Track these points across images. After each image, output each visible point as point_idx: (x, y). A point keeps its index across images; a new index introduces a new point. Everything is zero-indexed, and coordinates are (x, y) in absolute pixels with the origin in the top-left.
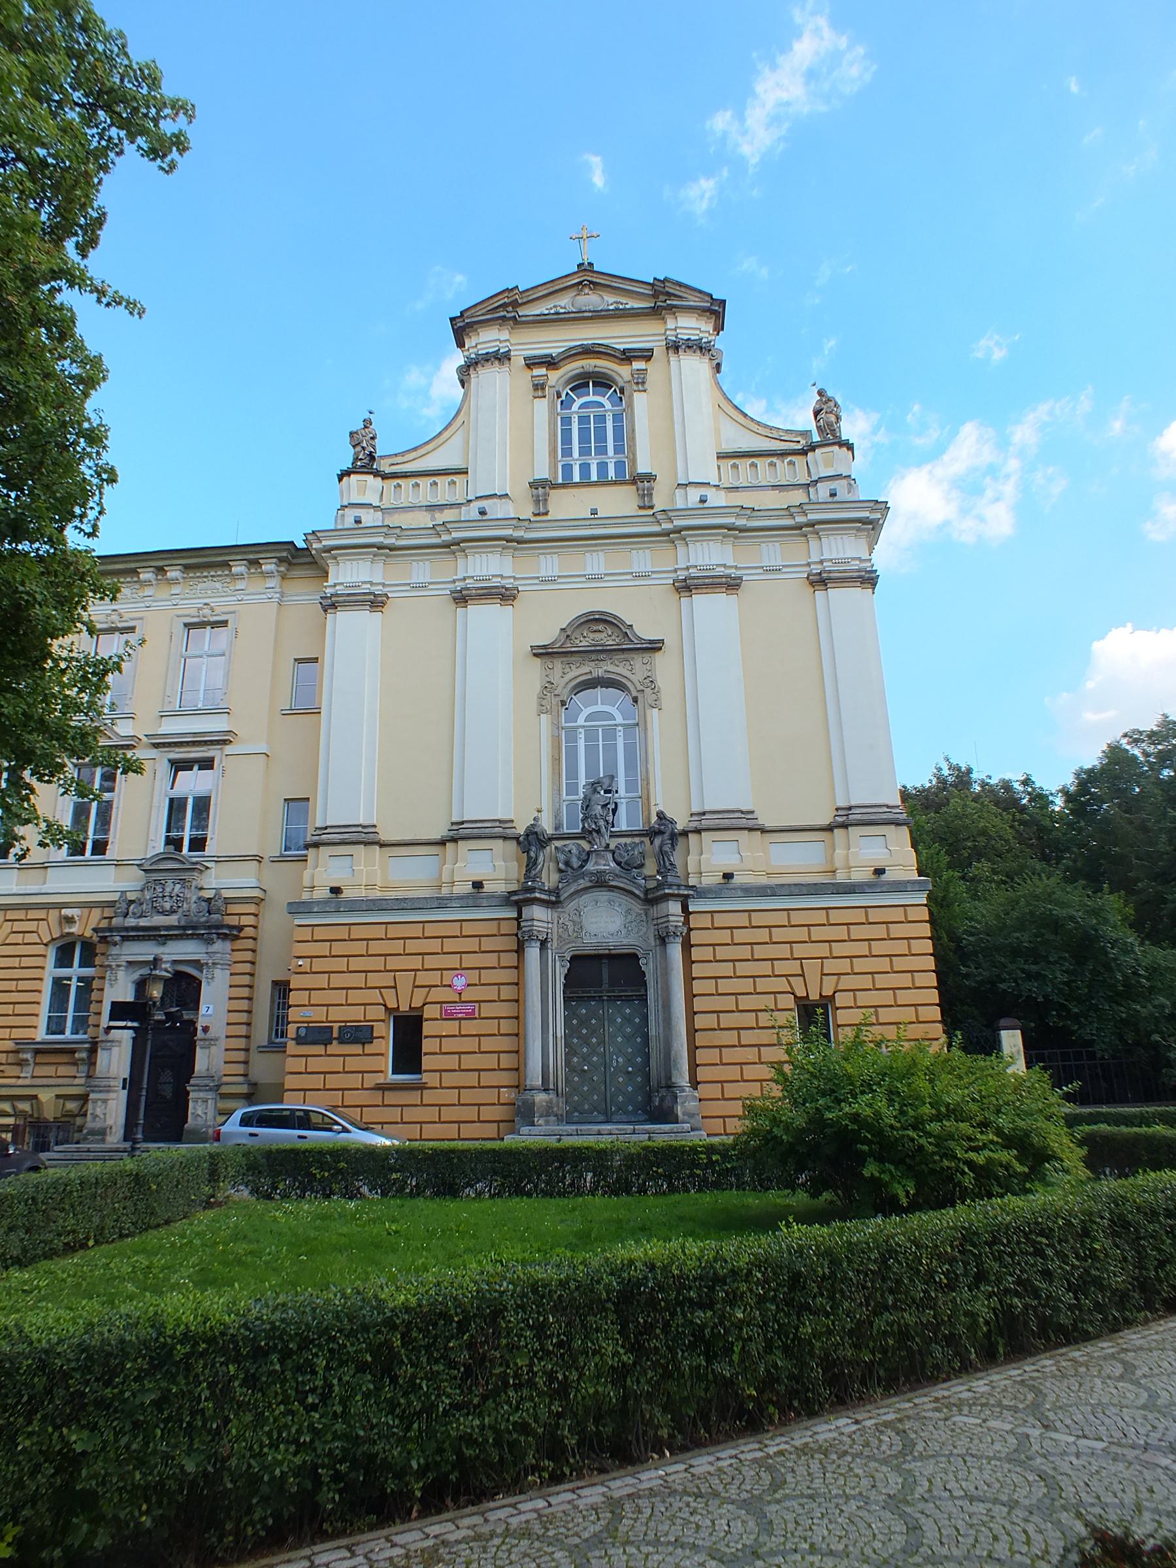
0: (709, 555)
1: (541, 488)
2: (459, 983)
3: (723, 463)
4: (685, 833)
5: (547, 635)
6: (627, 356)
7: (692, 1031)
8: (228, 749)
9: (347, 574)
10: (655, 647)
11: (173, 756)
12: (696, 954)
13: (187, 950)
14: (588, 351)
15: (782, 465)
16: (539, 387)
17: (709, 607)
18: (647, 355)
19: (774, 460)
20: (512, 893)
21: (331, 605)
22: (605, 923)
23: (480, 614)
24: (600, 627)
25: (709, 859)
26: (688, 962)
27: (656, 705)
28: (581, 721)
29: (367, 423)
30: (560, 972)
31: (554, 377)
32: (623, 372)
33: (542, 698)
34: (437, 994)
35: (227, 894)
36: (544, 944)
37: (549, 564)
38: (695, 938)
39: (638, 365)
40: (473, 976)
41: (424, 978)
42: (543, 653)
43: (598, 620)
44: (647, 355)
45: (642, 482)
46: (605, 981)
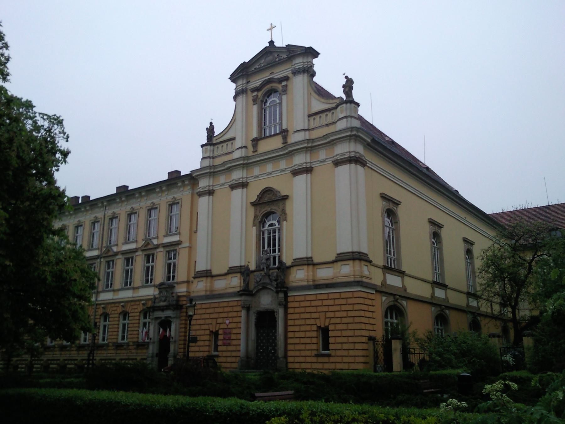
1: (256, 141)
2: (227, 322)
3: (312, 119)
4: (289, 267)
5: (254, 198)
6: (280, 81)
7: (286, 338)
8: (180, 246)
9: (203, 183)
10: (286, 198)
11: (167, 249)
12: (290, 311)
13: (169, 313)
14: (270, 81)
15: (329, 114)
16: (255, 101)
17: (302, 179)
18: (287, 79)
19: (327, 113)
20: (239, 292)
21: (200, 194)
22: (266, 301)
23: (238, 192)
24: (269, 193)
25: (299, 276)
26: (286, 313)
28: (266, 227)
29: (211, 123)
30: (253, 318)
31: (260, 94)
32: (279, 87)
33: (254, 221)
34: (222, 326)
35: (179, 294)
36: (248, 309)
37: (256, 171)
38: (290, 305)
39: (284, 83)
40: (231, 320)
41: (220, 321)
42: (254, 204)
43: (267, 191)
45: (284, 133)
46: (265, 321)
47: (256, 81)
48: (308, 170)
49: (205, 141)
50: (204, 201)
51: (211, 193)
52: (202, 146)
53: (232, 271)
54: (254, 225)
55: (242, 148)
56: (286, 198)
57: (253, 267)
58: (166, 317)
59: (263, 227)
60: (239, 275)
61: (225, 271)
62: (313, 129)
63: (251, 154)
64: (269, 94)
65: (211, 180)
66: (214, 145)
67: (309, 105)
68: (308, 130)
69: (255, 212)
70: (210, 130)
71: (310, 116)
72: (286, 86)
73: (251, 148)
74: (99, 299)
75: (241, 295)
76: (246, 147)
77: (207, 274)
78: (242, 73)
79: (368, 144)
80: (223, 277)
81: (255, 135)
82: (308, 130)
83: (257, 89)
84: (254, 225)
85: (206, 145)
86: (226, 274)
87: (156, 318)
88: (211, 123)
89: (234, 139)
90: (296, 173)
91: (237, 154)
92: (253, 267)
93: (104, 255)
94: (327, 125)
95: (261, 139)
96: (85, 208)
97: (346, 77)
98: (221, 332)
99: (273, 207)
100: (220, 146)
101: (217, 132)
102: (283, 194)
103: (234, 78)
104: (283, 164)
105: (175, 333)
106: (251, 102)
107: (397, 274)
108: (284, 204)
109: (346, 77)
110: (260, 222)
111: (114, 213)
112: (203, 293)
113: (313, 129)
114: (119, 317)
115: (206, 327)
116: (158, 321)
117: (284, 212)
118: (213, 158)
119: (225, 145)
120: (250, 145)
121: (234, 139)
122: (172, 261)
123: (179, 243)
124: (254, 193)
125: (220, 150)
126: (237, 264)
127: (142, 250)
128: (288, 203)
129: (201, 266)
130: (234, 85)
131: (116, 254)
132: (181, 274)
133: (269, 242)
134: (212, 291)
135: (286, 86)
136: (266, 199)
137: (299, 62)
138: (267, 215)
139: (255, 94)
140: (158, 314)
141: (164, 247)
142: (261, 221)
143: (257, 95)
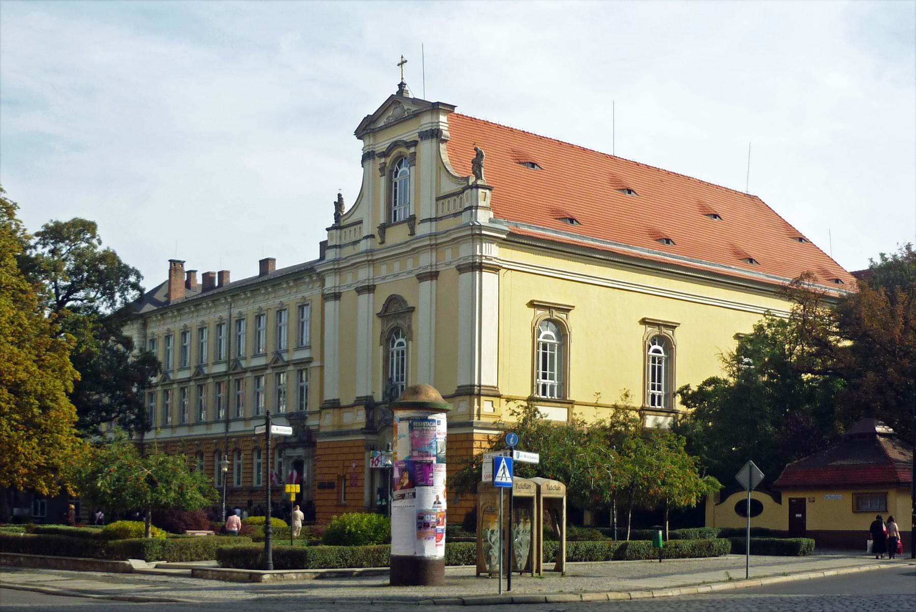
0: (426, 260)
1: (383, 228)
2: (354, 465)
5: (379, 309)
8: (312, 365)
13: (300, 452)
14: (395, 145)
16: (382, 169)
18: (415, 143)
19: (455, 197)
23: (364, 298)
27: (411, 339)
29: (339, 195)
31: (388, 160)
34: (350, 470)
37: (383, 270)
39: (412, 150)
42: (379, 315)
43: (393, 300)
44: (415, 143)
47: (382, 143)
48: (433, 275)
49: (331, 222)
50: (330, 306)
51: (337, 296)
52: (328, 229)
53: (359, 402)
54: (381, 344)
55: (367, 237)
56: (412, 310)
57: (378, 398)
58: (298, 456)
59: (393, 346)
60: (362, 407)
61: (351, 402)
62: (441, 218)
63: (378, 247)
64: (399, 161)
65: (338, 277)
66: (341, 228)
67: (438, 185)
68: (436, 219)
69: (383, 326)
70: (339, 205)
71: (438, 199)
72: (415, 153)
73: (378, 239)
74: (230, 430)
75: (364, 433)
76: (372, 236)
77: (334, 405)
78: (366, 129)
79: (504, 240)
80: (350, 409)
81: (382, 220)
82: (436, 219)
83: (384, 155)
84: (381, 344)
85: (334, 228)
86: (352, 406)
87: (290, 457)
88: (339, 195)
89: (361, 222)
90: (421, 278)
91: (364, 246)
92: (378, 398)
93: (231, 372)
94: (456, 215)
95: (389, 226)
96: (207, 304)
97: (476, 149)
98: (348, 477)
99: (400, 322)
100: (347, 230)
101: (348, 206)
102: (410, 304)
103: (361, 132)
104: (410, 264)
105: (308, 475)
106: (379, 173)
107: (559, 405)
108: (410, 318)
109: (476, 149)
110: (388, 340)
111: (240, 313)
112: (329, 430)
113: (441, 218)
114: (252, 455)
115: (333, 470)
116: (292, 461)
117: (409, 327)
118: (340, 247)
119: (352, 228)
120: (376, 232)
121: (361, 222)
122: (304, 384)
123: (309, 361)
124: (381, 297)
125: (350, 235)
126: (362, 392)
127: (272, 368)
128: (414, 314)
129: (329, 395)
130: (361, 144)
131: (245, 371)
132: (313, 404)
133: (394, 367)
134: (340, 426)
135: (415, 153)
136: (392, 310)
137: (426, 122)
138: (396, 331)
139: (383, 160)
140: (289, 452)
141: (294, 364)
142: (388, 339)
143: (385, 163)
